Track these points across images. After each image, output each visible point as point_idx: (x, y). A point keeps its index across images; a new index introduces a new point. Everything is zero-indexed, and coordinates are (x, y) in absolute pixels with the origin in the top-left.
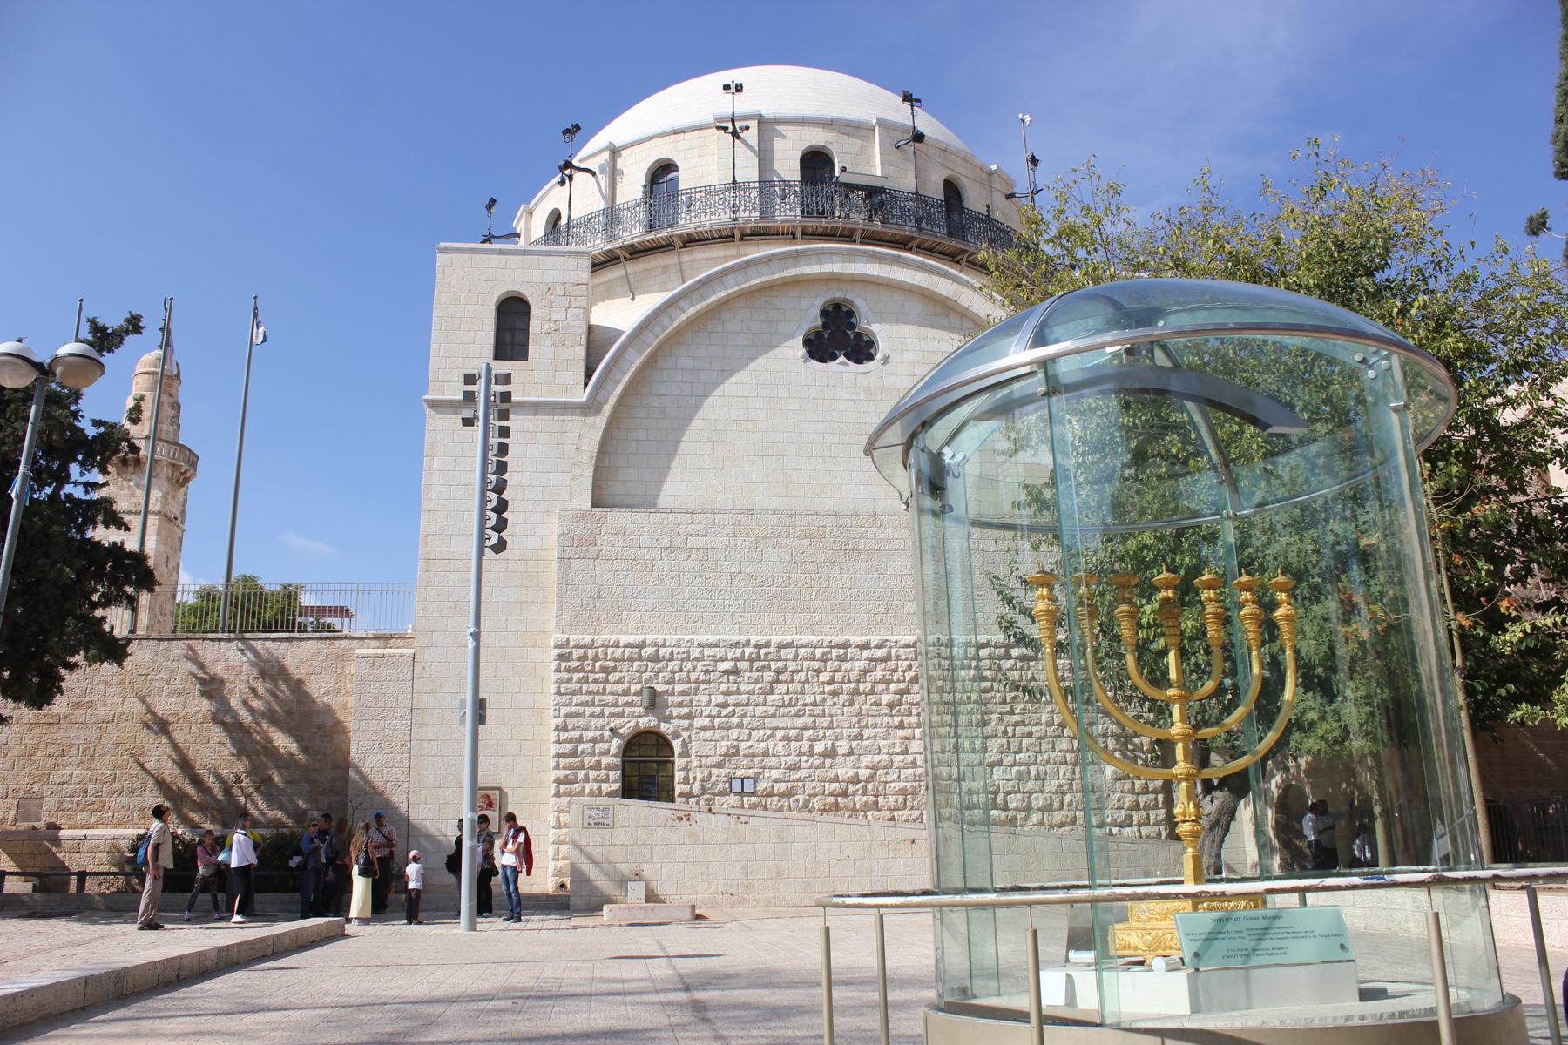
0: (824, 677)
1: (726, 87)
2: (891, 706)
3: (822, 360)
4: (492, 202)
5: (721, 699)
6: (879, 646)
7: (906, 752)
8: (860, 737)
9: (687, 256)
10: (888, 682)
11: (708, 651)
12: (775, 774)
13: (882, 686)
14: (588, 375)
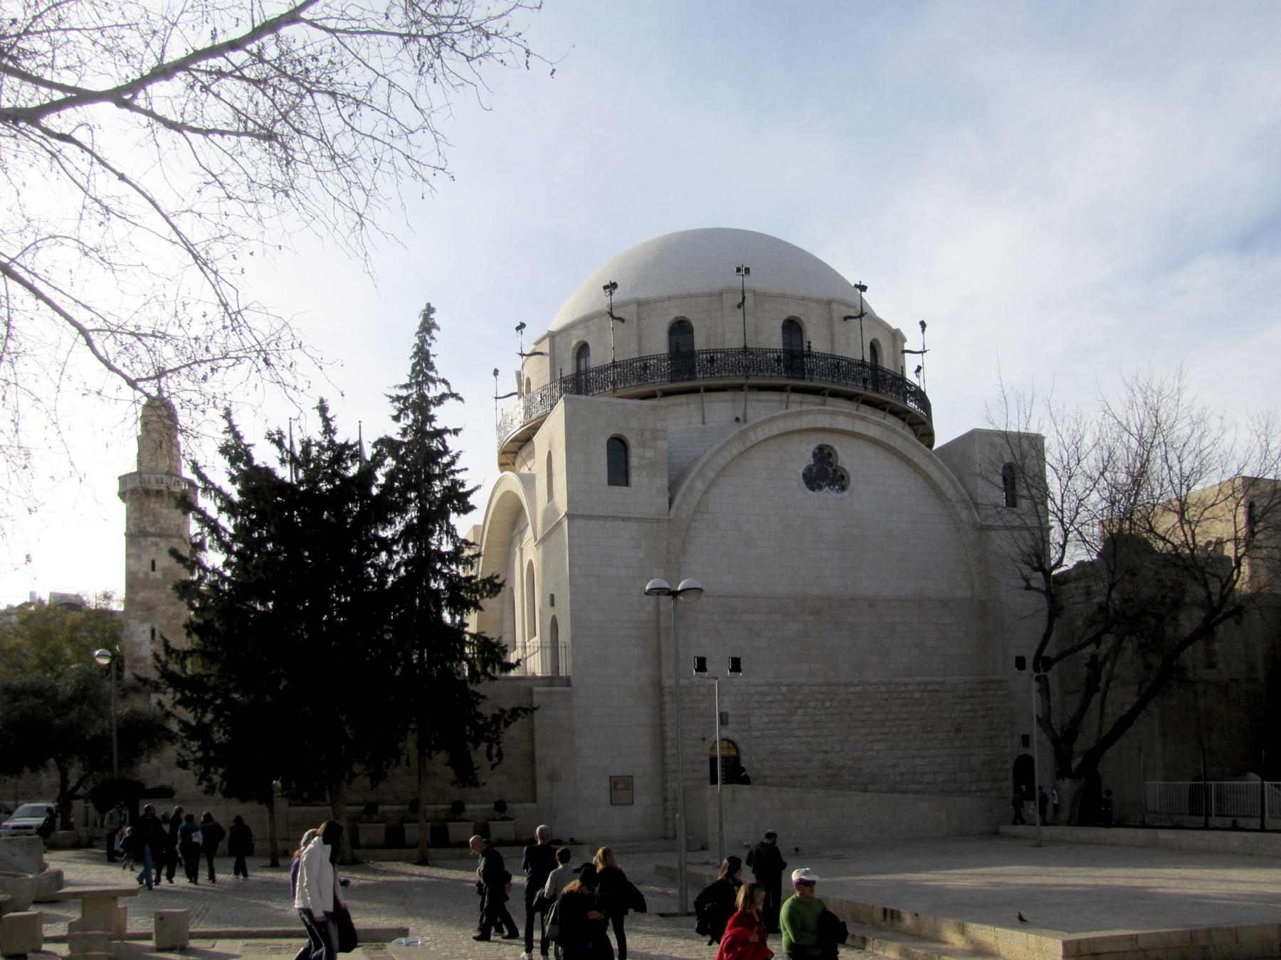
0: (828, 704)
2: (864, 721)
3: (813, 489)
5: (766, 719)
6: (856, 685)
7: (871, 750)
9: (707, 396)
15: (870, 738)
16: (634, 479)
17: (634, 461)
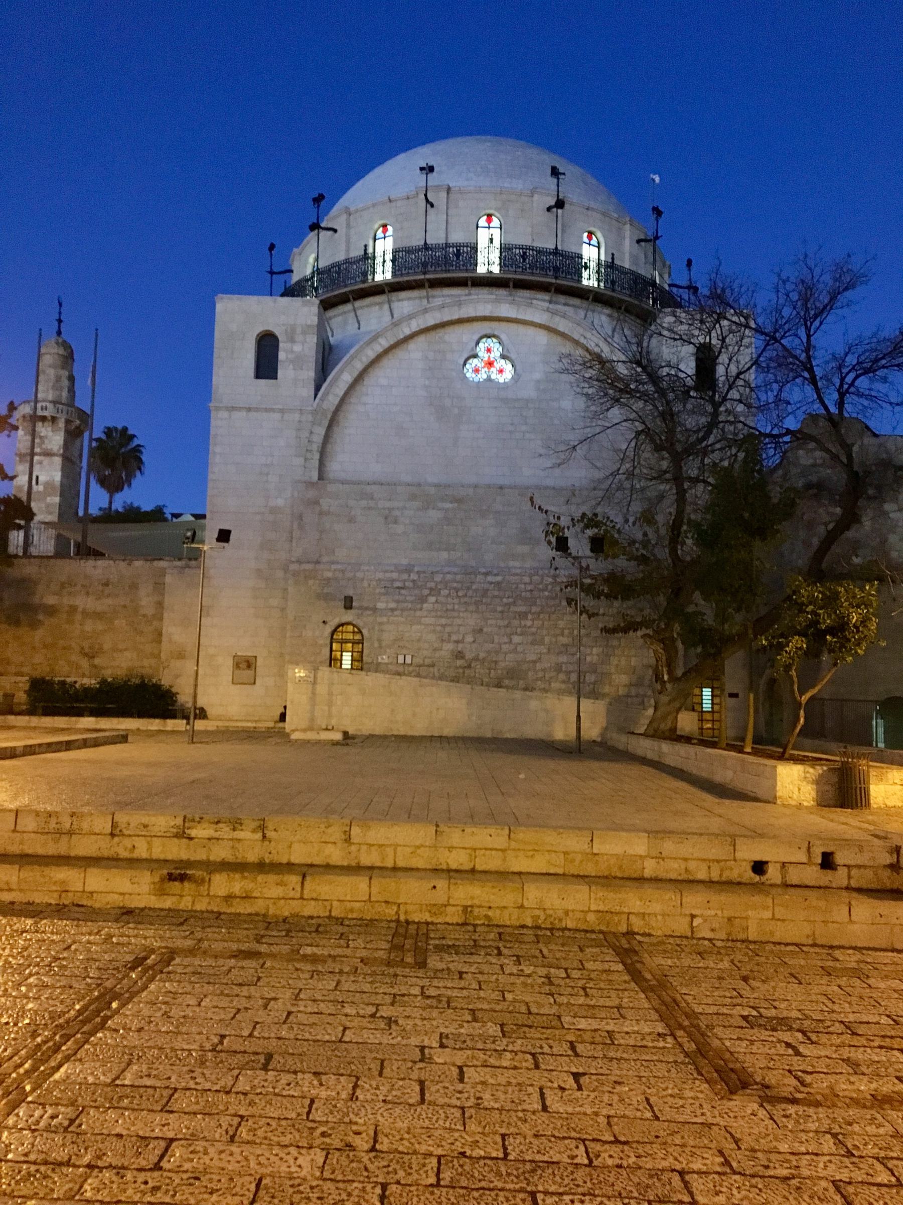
1: (422, 169)
2: (502, 612)
4: (272, 247)
8: (481, 631)
10: (501, 598)
11: (388, 575)
12: (425, 653)
13: (498, 600)
14: (318, 388)
15: (508, 630)
16: (280, 373)
17: (282, 355)
